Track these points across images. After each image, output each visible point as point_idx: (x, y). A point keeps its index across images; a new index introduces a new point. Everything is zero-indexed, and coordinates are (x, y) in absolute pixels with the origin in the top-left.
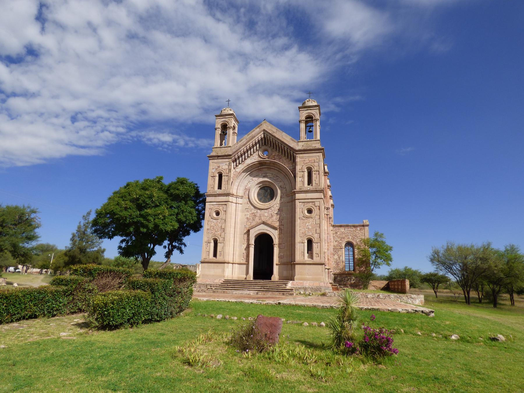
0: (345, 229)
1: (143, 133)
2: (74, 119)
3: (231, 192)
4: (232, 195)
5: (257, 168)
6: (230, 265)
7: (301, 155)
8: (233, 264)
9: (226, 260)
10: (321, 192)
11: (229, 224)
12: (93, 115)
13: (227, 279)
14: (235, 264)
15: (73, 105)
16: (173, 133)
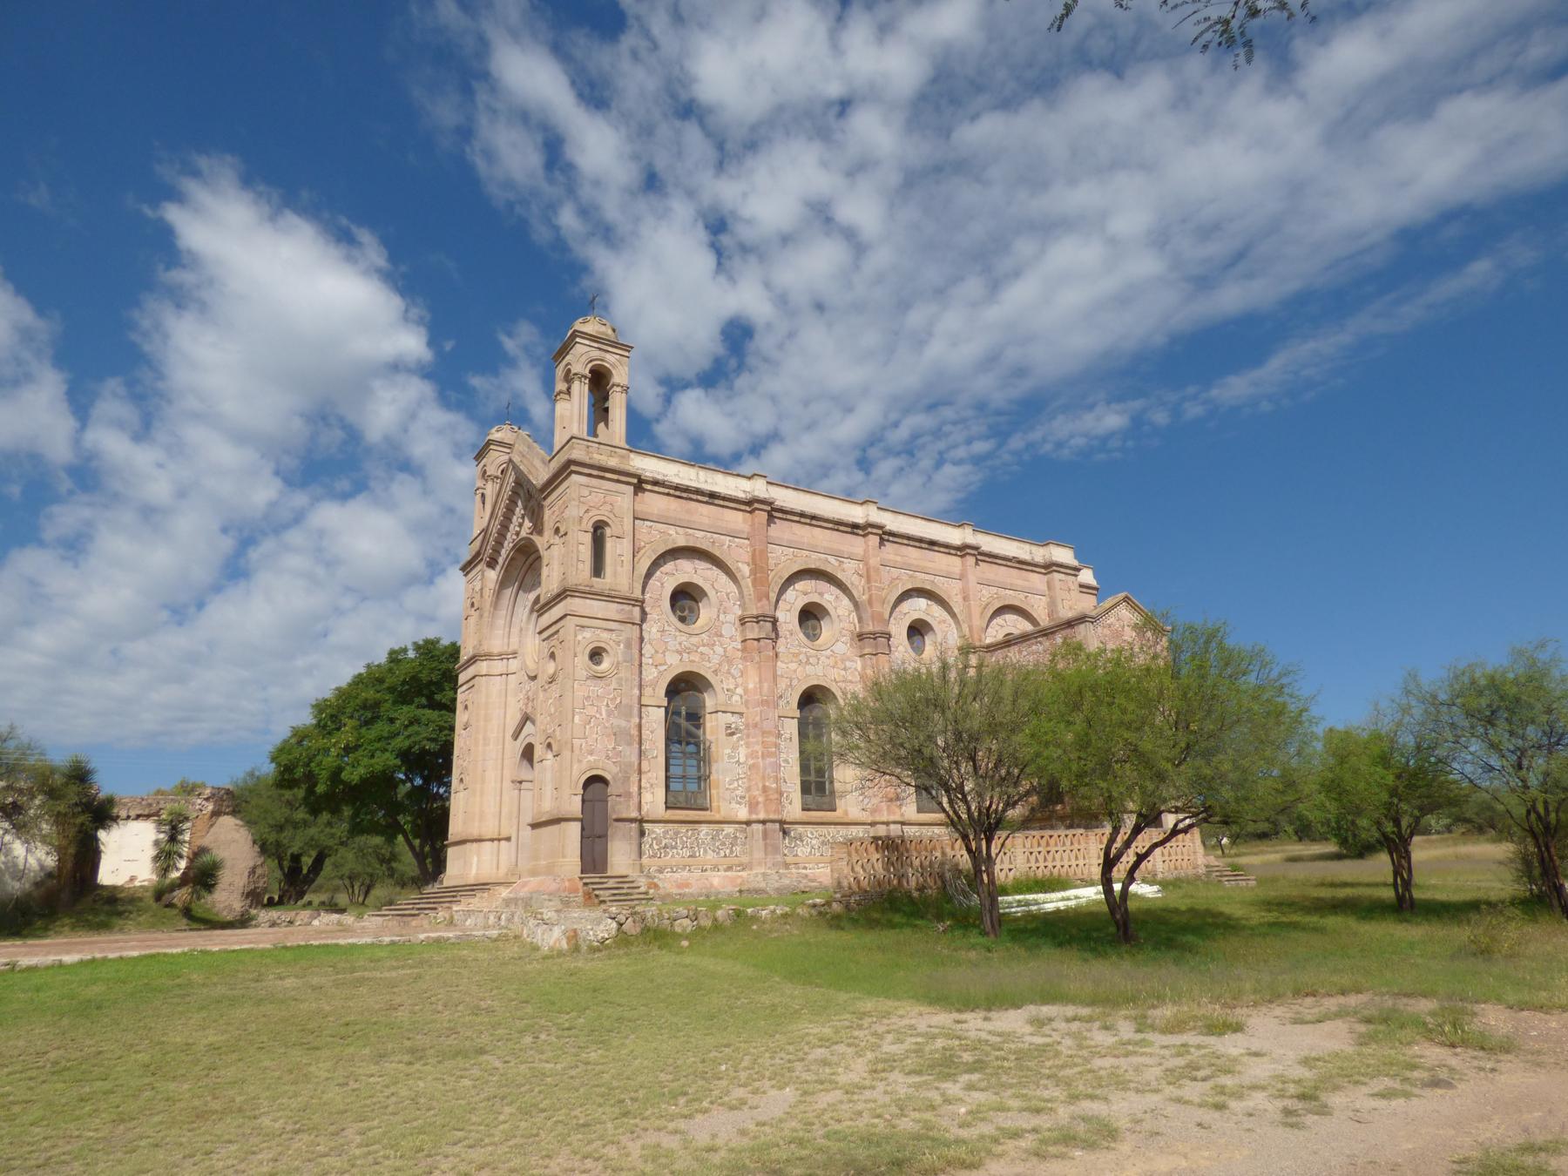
0: (1020, 652)
1: (1036, 435)
2: (864, 464)
3: (485, 648)
4: (488, 656)
5: (524, 569)
6: (488, 844)
7: (549, 500)
8: (492, 840)
9: (474, 832)
10: (566, 597)
11: (481, 737)
12: (903, 433)
13: (472, 882)
14: (499, 840)
15: (850, 429)
16: (1120, 399)
